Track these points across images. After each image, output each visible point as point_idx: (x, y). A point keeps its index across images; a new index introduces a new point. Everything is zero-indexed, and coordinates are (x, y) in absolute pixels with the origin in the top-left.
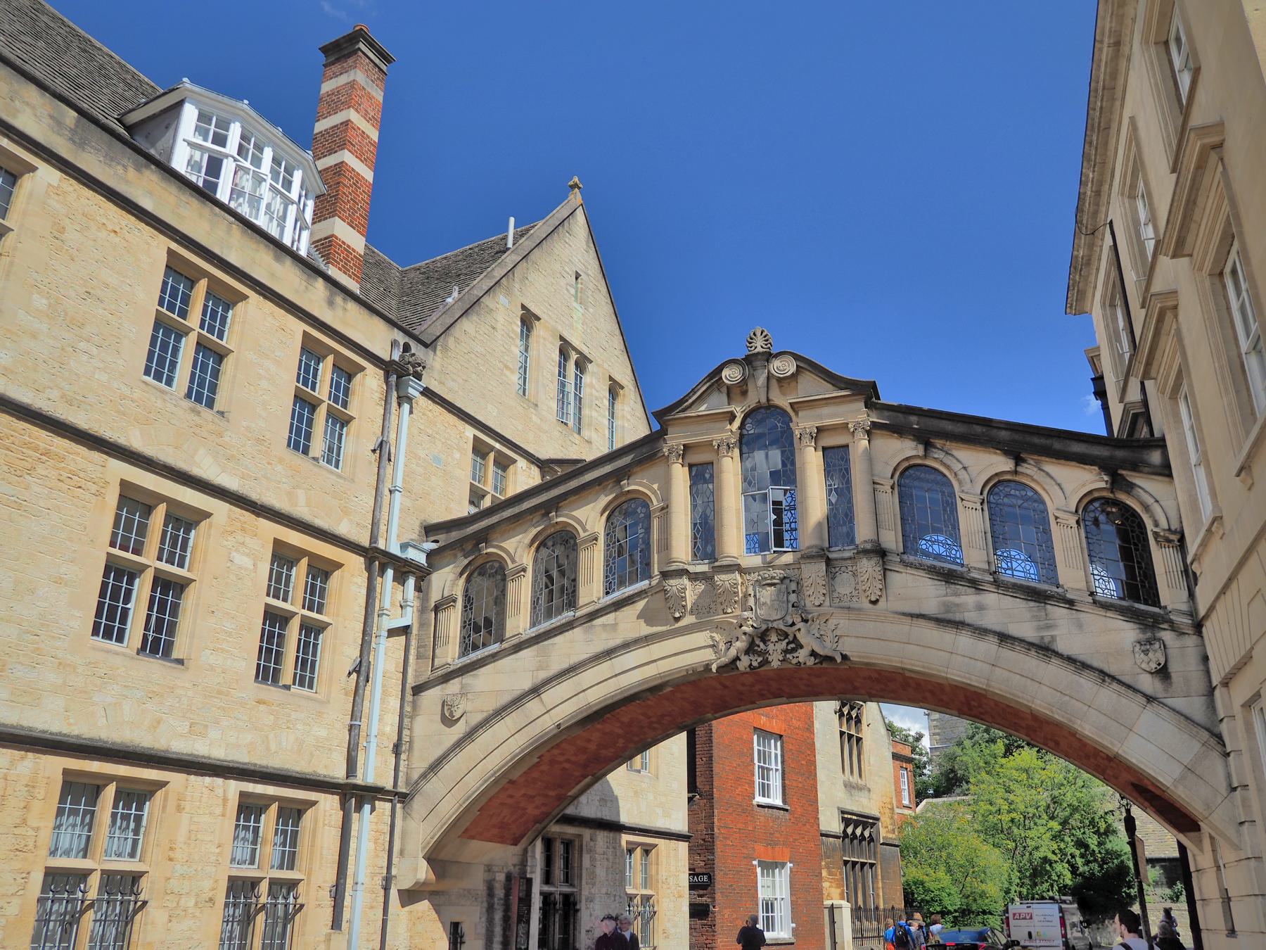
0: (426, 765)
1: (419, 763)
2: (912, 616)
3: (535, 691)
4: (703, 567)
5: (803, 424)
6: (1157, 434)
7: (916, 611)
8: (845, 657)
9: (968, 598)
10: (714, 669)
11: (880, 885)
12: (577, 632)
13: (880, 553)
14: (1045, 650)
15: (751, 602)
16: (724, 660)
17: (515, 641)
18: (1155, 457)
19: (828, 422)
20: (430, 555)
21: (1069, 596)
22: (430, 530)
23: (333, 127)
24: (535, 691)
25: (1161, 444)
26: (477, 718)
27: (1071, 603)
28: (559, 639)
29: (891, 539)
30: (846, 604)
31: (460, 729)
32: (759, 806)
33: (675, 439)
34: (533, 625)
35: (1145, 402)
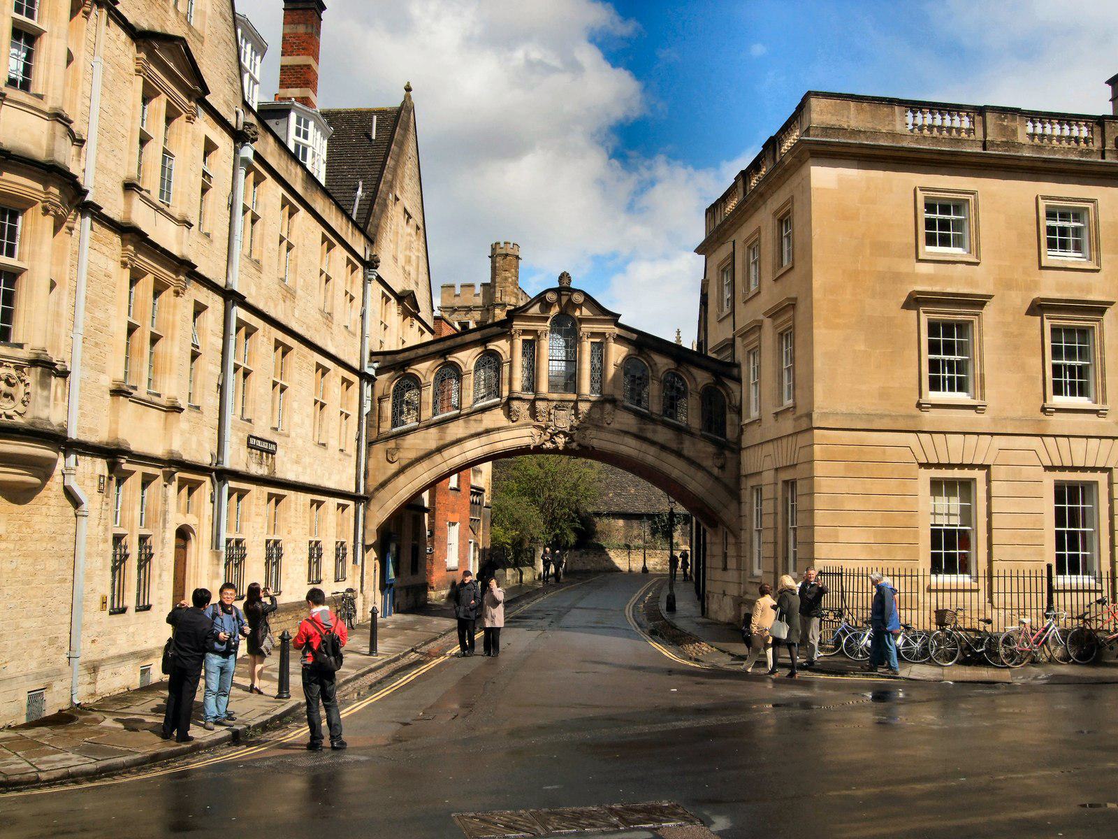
0: (376, 484)
1: (373, 484)
2: (626, 433)
3: (439, 450)
4: (530, 396)
5: (585, 328)
6: (736, 362)
7: (627, 430)
8: (593, 448)
9: (651, 427)
10: (532, 448)
11: (481, 533)
12: (461, 422)
13: (613, 401)
14: (679, 454)
15: (552, 417)
16: (537, 444)
17: (427, 423)
18: (735, 371)
19: (595, 330)
20: (379, 371)
21: (693, 430)
22: (373, 354)
23: (297, 66)
24: (439, 450)
25: (738, 366)
26: (404, 462)
27: (692, 434)
28: (451, 425)
29: (619, 395)
30: (595, 423)
31: (394, 468)
32: (451, 489)
33: (518, 325)
34: (434, 415)
35: (733, 339)
